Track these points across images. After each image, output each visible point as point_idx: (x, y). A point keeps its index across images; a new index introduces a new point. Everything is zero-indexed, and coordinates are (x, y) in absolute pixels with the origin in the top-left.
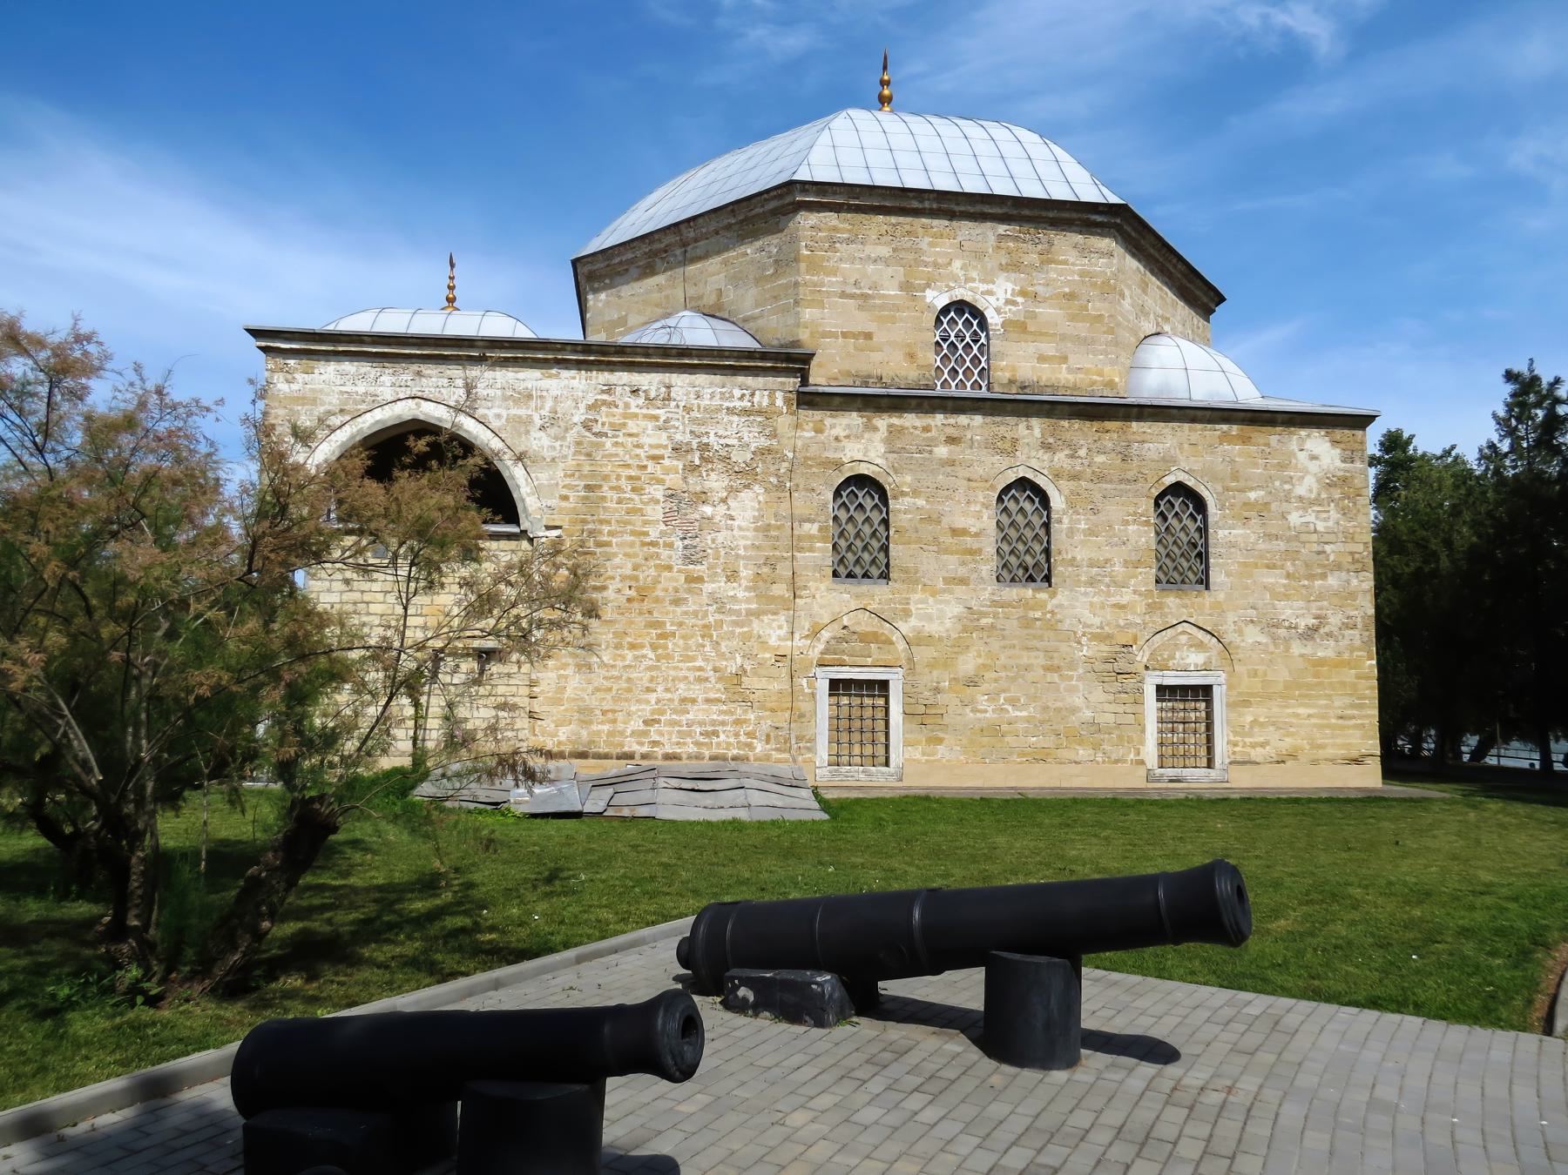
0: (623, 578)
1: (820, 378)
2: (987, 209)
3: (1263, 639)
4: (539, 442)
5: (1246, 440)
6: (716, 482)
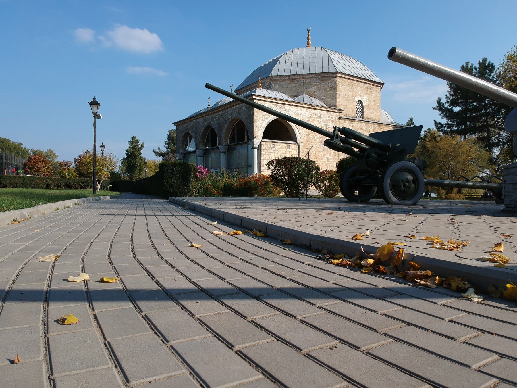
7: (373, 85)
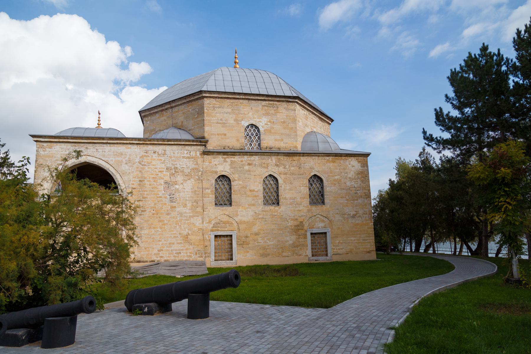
0: (151, 208)
1: (210, 147)
2: (259, 98)
3: (341, 219)
4: (125, 167)
5: (333, 162)
6: (179, 178)
7: (278, 101)
